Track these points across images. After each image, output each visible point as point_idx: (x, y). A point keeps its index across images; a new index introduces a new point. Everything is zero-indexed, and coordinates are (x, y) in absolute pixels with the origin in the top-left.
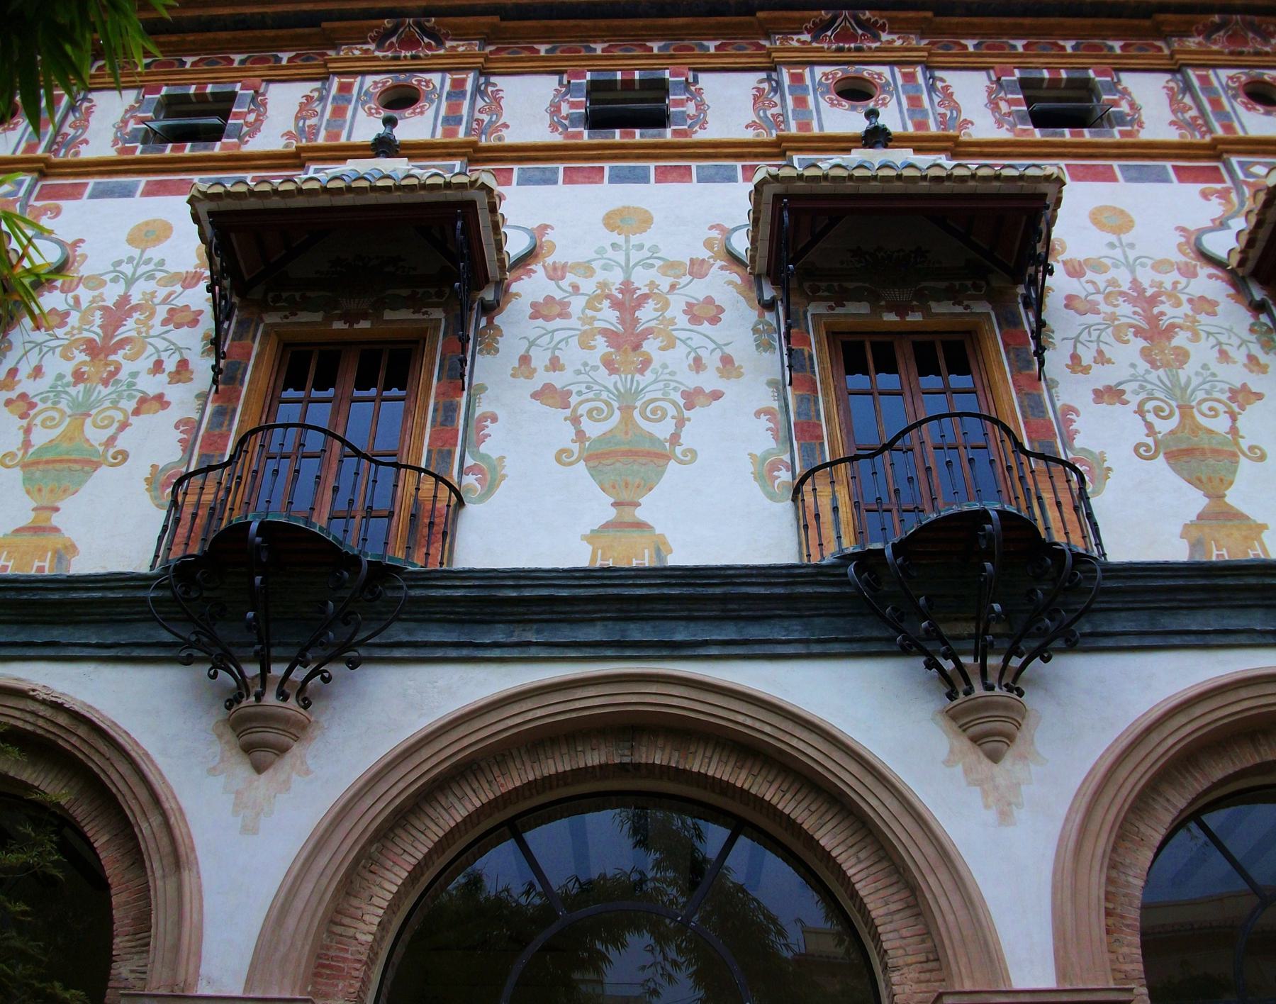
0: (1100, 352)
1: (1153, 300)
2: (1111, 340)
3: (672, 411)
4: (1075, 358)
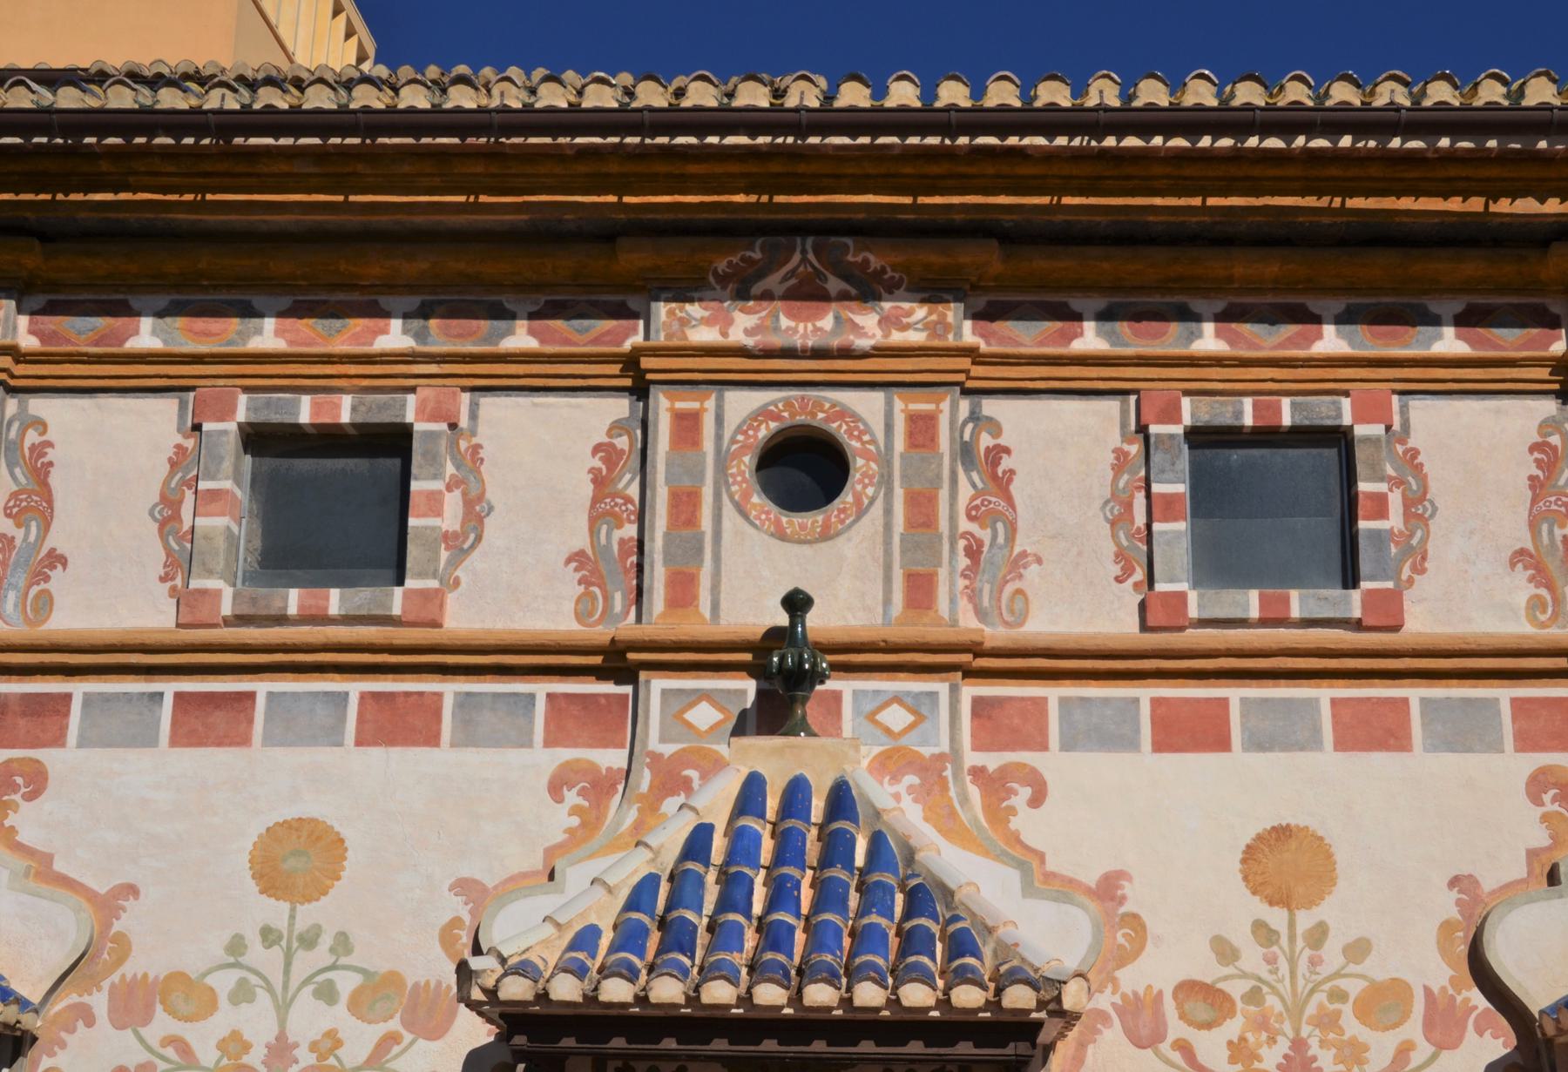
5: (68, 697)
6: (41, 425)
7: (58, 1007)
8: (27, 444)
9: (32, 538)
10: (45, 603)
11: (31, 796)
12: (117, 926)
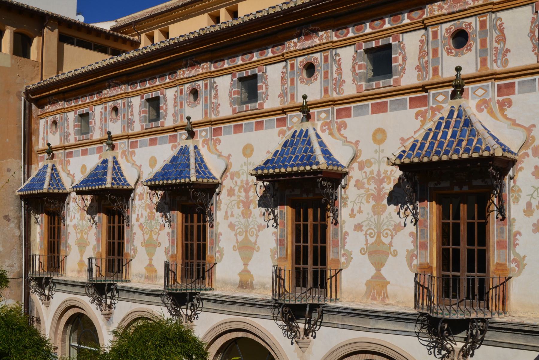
0: (360, 208)
1: (381, 181)
2: (364, 201)
3: (255, 233)
4: (352, 210)
5: (514, 83)
6: (500, 19)
7: (521, 153)
8: (498, 24)
9: (502, 47)
10: (507, 61)
11: (509, 107)
12: (532, 134)
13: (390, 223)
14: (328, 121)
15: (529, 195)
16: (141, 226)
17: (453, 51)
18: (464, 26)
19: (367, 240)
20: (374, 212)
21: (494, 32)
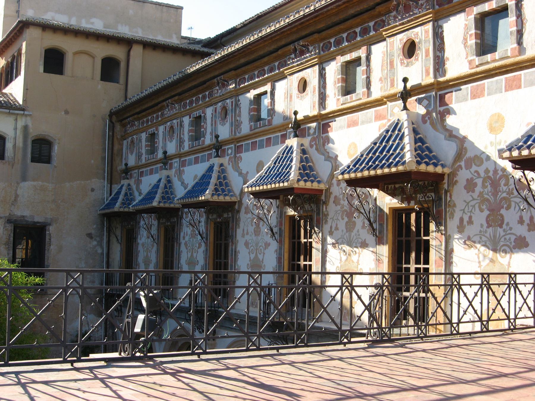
0: (337, 225)
2: (340, 218)
4: (331, 227)
12: (465, 145)
13: (358, 241)
14: (315, 136)
15: (462, 210)
16: (186, 244)
17: (405, 62)
18: (413, 36)
19: (341, 257)
20: (347, 229)
21: (436, 40)
